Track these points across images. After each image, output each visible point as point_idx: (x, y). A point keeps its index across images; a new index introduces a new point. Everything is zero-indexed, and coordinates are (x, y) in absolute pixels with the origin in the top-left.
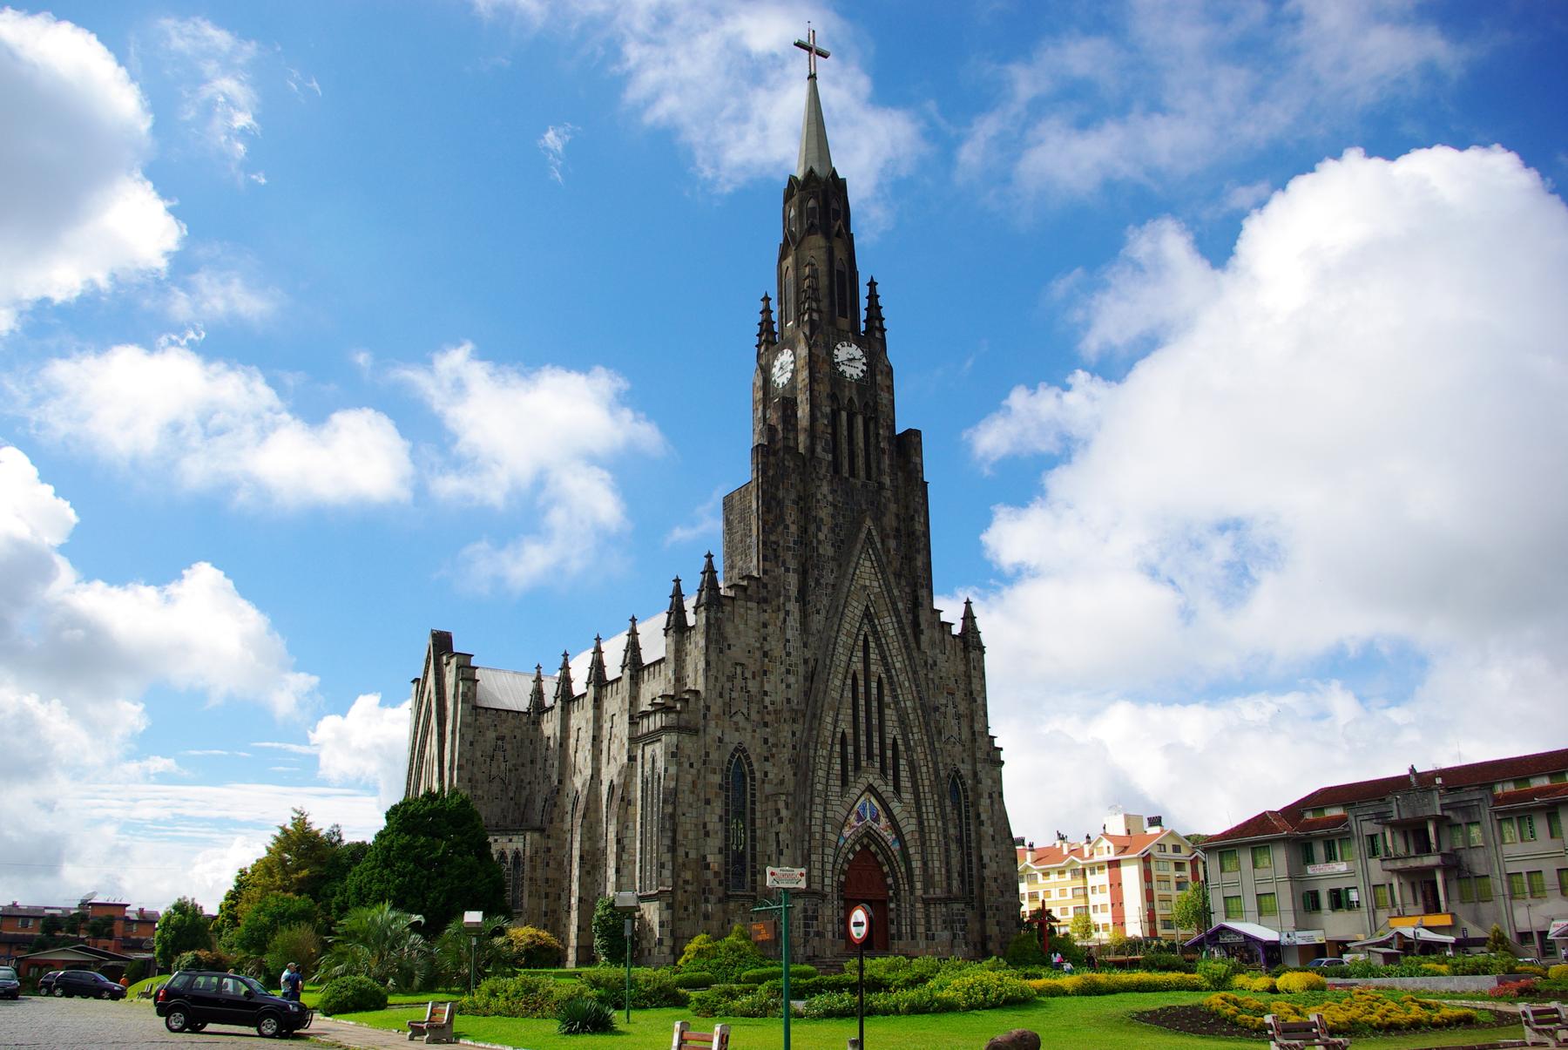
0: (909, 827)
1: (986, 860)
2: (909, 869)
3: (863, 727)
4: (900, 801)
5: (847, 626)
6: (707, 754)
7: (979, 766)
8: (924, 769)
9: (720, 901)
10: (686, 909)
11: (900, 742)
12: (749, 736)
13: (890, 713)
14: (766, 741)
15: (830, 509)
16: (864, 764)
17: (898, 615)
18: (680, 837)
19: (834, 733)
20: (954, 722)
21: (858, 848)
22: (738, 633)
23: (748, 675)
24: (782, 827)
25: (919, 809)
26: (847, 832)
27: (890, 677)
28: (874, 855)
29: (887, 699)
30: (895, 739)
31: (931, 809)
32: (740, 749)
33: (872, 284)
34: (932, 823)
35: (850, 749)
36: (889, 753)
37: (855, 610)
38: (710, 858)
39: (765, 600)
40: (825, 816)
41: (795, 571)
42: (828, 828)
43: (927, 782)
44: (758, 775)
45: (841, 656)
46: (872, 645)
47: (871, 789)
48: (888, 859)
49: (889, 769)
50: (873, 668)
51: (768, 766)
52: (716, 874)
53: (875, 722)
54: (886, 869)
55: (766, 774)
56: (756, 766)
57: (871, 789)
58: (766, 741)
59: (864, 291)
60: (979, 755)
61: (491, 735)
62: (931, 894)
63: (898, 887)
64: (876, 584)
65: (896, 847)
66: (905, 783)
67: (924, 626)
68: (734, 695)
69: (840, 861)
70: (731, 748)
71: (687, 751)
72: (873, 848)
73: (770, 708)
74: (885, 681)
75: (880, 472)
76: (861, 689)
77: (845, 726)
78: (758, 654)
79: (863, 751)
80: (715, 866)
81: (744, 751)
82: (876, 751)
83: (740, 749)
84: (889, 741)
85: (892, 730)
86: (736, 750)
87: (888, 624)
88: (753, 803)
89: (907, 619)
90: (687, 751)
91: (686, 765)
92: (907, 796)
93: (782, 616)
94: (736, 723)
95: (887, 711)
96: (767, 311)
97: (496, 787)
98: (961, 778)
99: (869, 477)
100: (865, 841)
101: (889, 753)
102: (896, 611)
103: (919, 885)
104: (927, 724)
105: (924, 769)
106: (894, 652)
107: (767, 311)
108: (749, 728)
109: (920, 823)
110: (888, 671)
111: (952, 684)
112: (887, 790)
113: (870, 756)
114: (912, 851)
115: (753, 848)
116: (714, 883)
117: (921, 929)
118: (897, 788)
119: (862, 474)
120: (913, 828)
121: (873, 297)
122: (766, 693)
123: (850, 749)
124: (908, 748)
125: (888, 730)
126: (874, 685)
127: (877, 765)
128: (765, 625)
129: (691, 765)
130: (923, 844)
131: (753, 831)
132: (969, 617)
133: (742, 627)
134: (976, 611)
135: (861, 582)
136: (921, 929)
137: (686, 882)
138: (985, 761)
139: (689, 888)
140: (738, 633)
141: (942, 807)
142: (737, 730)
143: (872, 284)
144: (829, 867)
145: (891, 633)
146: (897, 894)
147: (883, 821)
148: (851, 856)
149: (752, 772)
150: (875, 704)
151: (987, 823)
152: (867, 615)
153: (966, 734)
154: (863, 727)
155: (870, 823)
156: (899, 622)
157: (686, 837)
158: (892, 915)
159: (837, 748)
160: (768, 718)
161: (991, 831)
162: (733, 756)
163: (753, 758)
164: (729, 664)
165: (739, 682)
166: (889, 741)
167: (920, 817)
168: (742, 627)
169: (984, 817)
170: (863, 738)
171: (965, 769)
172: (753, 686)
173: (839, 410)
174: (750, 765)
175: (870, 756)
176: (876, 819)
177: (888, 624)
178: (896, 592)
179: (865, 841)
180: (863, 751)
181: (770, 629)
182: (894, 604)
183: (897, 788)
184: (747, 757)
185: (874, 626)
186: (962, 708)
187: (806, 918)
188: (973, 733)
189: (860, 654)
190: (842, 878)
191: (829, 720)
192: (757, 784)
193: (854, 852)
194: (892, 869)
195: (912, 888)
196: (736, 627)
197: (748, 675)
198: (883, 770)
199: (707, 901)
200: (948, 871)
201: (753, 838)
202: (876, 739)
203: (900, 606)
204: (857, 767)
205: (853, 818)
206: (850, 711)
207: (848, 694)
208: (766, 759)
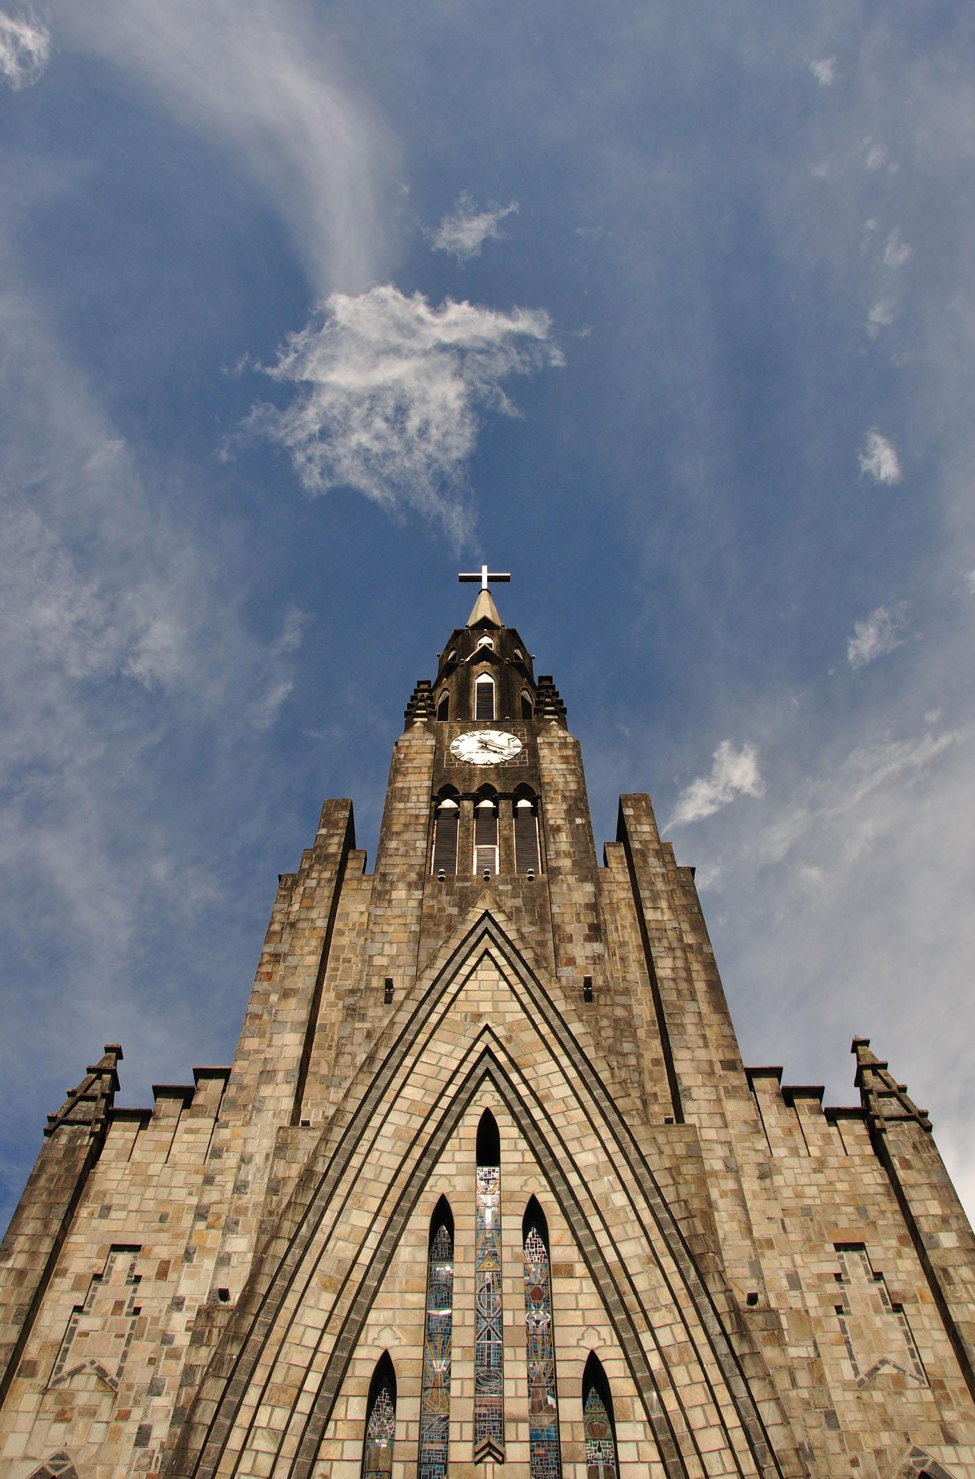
8: (711, 1440)
11: (614, 1369)
12: (98, 1432)
13: (576, 1293)
37: (444, 1055)
46: (507, 1129)
58: (143, 1436)
68: (85, 1323)
84: (571, 1371)
87: (549, 1076)
94: (65, 1399)
105: (711, 1440)
124: (645, 1383)
128: (216, 1153)
142: (62, 1417)
159: (353, 1407)
164: (92, 1250)
165: (115, 1288)
177: (549, 1076)
191: (313, 1317)
202: (516, 1368)
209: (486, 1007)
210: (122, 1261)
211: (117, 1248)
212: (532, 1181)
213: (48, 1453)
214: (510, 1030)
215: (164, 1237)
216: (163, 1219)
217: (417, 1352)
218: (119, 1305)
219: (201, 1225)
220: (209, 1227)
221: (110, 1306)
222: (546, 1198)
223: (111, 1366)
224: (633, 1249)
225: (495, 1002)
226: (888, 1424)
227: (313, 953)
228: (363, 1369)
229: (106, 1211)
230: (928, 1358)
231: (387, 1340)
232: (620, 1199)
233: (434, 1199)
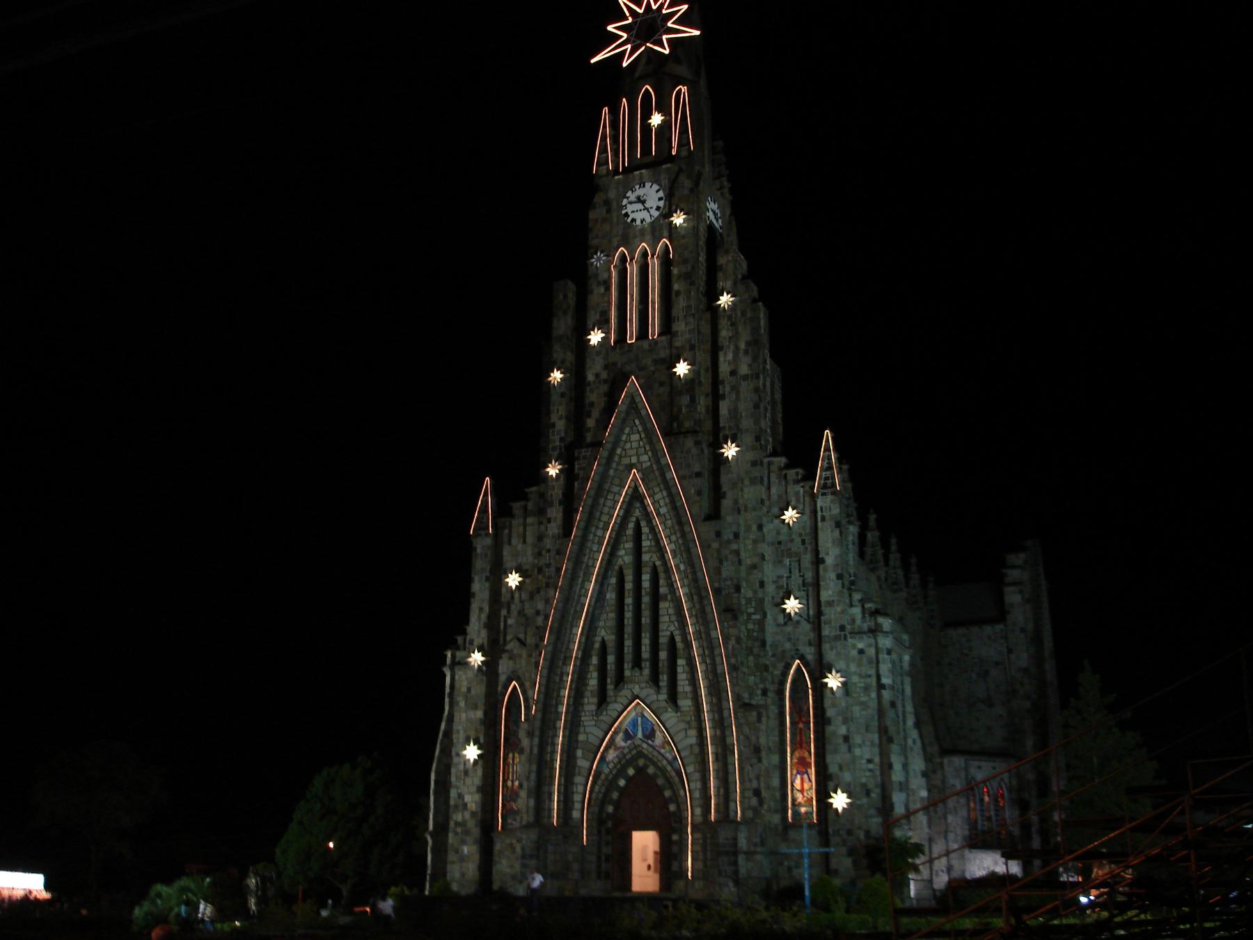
3: (629, 629)
11: (678, 639)
12: (524, 662)
16: (627, 673)
21: (631, 772)
29: (663, 590)
30: (672, 638)
35: (611, 659)
36: (663, 655)
38: (468, 798)
50: (645, 557)
53: (646, 620)
54: (667, 794)
66: (683, 685)
72: (651, 770)
74: (660, 569)
76: (629, 586)
77: (605, 633)
80: (473, 806)
82: (646, 654)
85: (667, 626)
95: (663, 605)
101: (663, 655)
113: (637, 663)
118: (673, 698)
120: (693, 740)
123: (611, 659)
125: (662, 626)
126: (646, 577)
127: (646, 672)
135: (626, 461)
150: (646, 599)
154: (629, 629)
159: (595, 660)
166: (663, 640)
168: (520, 547)
170: (628, 643)
175: (637, 663)
179: (641, 762)
183: (673, 698)
186: (809, 575)
189: (629, 545)
198: (655, 680)
202: (646, 641)
206: (612, 615)
207: (611, 596)
209: (634, 460)
217: (613, 637)
218: (519, 612)
222: (658, 563)
223: (521, 636)
225: (638, 456)
226: (789, 640)
227: (560, 418)
228: (597, 646)
231: (603, 633)
233: (616, 568)
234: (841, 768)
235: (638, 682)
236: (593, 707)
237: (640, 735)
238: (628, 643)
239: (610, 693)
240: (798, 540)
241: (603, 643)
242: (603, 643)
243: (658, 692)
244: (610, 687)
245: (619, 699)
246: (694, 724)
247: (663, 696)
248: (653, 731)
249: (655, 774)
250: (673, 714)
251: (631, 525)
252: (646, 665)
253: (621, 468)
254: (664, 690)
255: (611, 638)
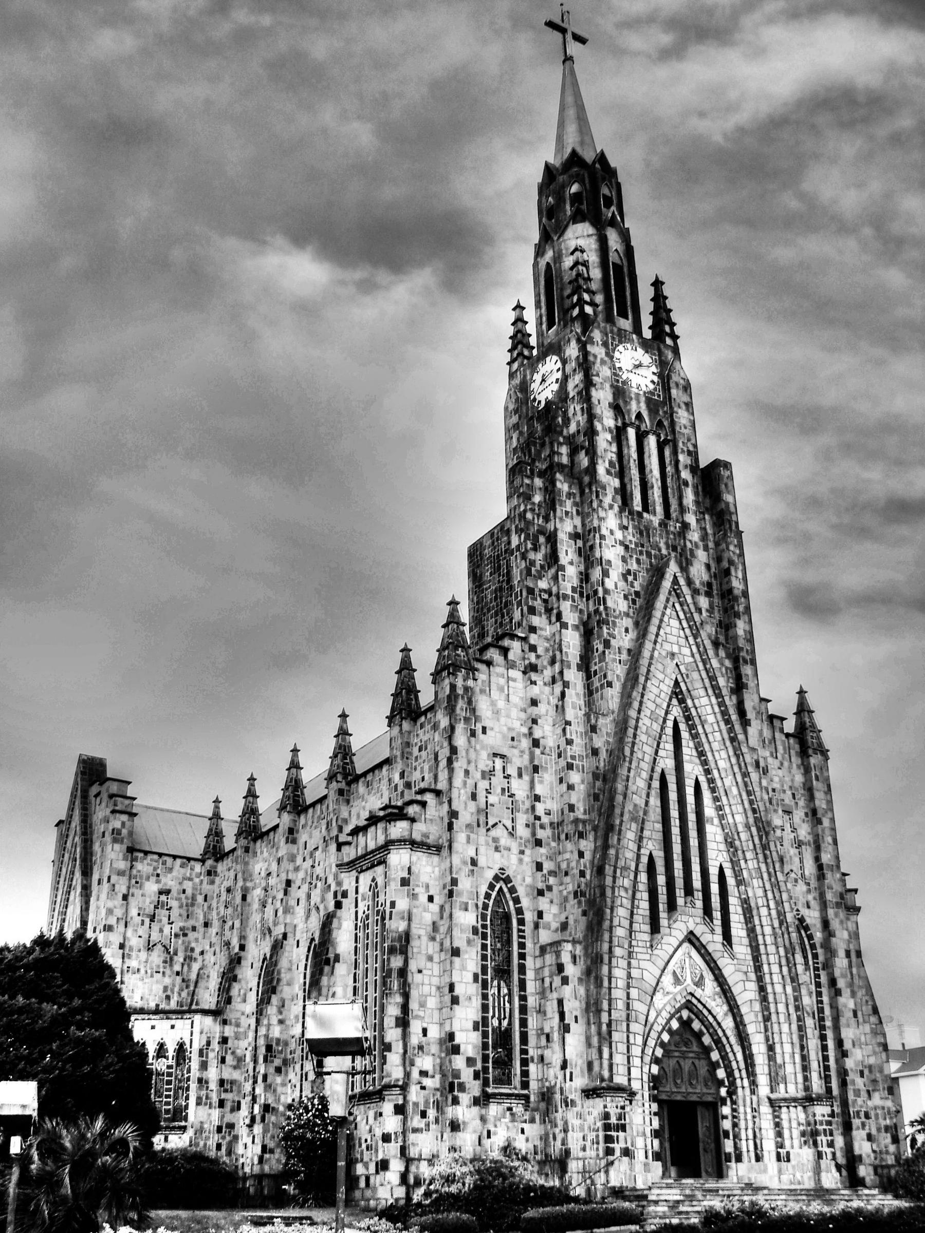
0: (746, 994)
1: (847, 1045)
2: (749, 1059)
3: (677, 849)
4: (733, 957)
5: (652, 706)
6: (454, 882)
7: (831, 912)
8: (764, 911)
9: (476, 1102)
10: (424, 1115)
11: (728, 873)
12: (514, 859)
13: (713, 832)
14: (539, 867)
15: (620, 550)
16: (680, 901)
17: (719, 695)
18: (413, 1005)
19: (638, 856)
20: (793, 851)
21: (675, 1025)
22: (497, 712)
23: (512, 771)
24: (567, 991)
25: (758, 968)
26: (660, 1000)
27: (711, 781)
28: (698, 1036)
29: (709, 811)
30: (721, 869)
31: (775, 969)
32: (502, 877)
33: (657, 284)
34: (779, 988)
35: (661, 880)
36: (715, 888)
39: (533, 668)
40: (629, 976)
41: (576, 627)
42: (634, 993)
43: (768, 930)
44: (529, 917)
45: (644, 749)
46: (685, 735)
47: (691, 938)
48: (718, 1042)
49: (716, 910)
51: (543, 903)
52: (470, 1061)
53: (694, 842)
54: (715, 1056)
55: (540, 915)
56: (525, 903)
57: (691, 938)
58: (539, 867)
59: (646, 294)
60: (829, 896)
61: (152, 887)
62: (781, 1093)
63: (732, 1083)
64: (686, 651)
65: (728, 1024)
66: (738, 930)
67: (751, 715)
68: (492, 799)
69: (651, 1042)
70: (489, 875)
71: (424, 878)
72: (696, 1025)
73: (545, 820)
74: (704, 786)
75: (682, 509)
76: (673, 796)
78: (525, 743)
79: (679, 883)
81: (507, 880)
82: (697, 883)
83: (502, 877)
86: (497, 878)
87: (705, 705)
88: (522, 956)
89: (731, 702)
90: (424, 878)
91: (423, 898)
92: (742, 949)
93: (558, 688)
94: (495, 840)
96: (519, 321)
97: (157, 957)
98: (807, 928)
99: (667, 514)
100: (685, 1014)
101: (715, 888)
102: (716, 689)
103: (763, 1080)
104: (765, 847)
105: (764, 911)
106: (716, 746)
107: (519, 321)
108: (515, 849)
109: (762, 989)
110: (708, 772)
111: (788, 798)
112: (713, 940)
114: (751, 1029)
115: (524, 1023)
116: (467, 1075)
117: (769, 1146)
119: (659, 509)
121: (659, 299)
122: (537, 798)
123: (661, 880)
124: (740, 882)
126: (690, 791)
127: (699, 904)
128: (534, 703)
129: (431, 899)
130: (767, 1019)
131: (523, 998)
132: (803, 709)
133: (501, 704)
134: (812, 701)
135: (667, 647)
136: (769, 1146)
137: (424, 1073)
138: (838, 905)
139: (427, 1082)
140: (497, 712)
141: (791, 965)
142: (497, 849)
143: (657, 284)
144: (636, 1051)
145: (711, 719)
146: (732, 1092)
147: (710, 984)
148: (666, 1037)
149: (520, 911)
151: (846, 992)
152: (678, 694)
153: (810, 868)
154: (677, 849)
155: (692, 988)
156: (721, 704)
157: (422, 1005)
158: (727, 1125)
159: (643, 877)
160: (541, 834)
161: (851, 1004)
162: (491, 887)
163: (521, 892)
164: (484, 755)
165: (498, 781)
166: (714, 872)
167: (760, 979)
168: (501, 704)
169: (841, 984)
170: (678, 865)
171: (813, 917)
172: (520, 787)
173: (625, 425)
174: (517, 900)
176: (700, 983)
177: (705, 705)
178: (715, 663)
179: (685, 1014)
180: (679, 883)
181: (542, 708)
182: (712, 678)
184: (513, 890)
185: (686, 709)
186: (804, 832)
187: (607, 1127)
188: (820, 867)
190: (655, 1069)
192: (528, 928)
193: (670, 1032)
194: (725, 1057)
195: (753, 1083)
196: (493, 703)
197: (512, 771)
199: (456, 1101)
200: (804, 1058)
201: (523, 1010)
203: (722, 682)
204: (672, 906)
205: (667, 979)
206: (659, 826)
207: (655, 801)
208: (541, 893)
209: (675, 649)
210: (499, 763)
211: (495, 755)
212: (696, 768)
213: (497, 867)
214: (687, 670)
215: (516, 752)
216: (513, 739)
217: (662, 854)
218: (503, 790)
219: (537, 751)
220: (542, 753)
221: (499, 791)
222: (702, 779)
224: (740, 819)
228: (645, 860)
229: (484, 730)
230: (807, 873)
232: (735, 791)
234: (854, 1045)
235: (690, 918)
236: (647, 937)
237: (689, 981)
238: (678, 865)
239: (664, 922)
240: (789, 793)
241: (651, 857)
242: (651, 857)
243: (712, 931)
244: (663, 915)
245: (674, 932)
246: (753, 976)
247: (719, 938)
248: (702, 976)
249: (701, 1031)
250: (730, 961)
251: (670, 724)
252: (699, 895)
253: (664, 653)
254: (719, 930)
255: (659, 855)
